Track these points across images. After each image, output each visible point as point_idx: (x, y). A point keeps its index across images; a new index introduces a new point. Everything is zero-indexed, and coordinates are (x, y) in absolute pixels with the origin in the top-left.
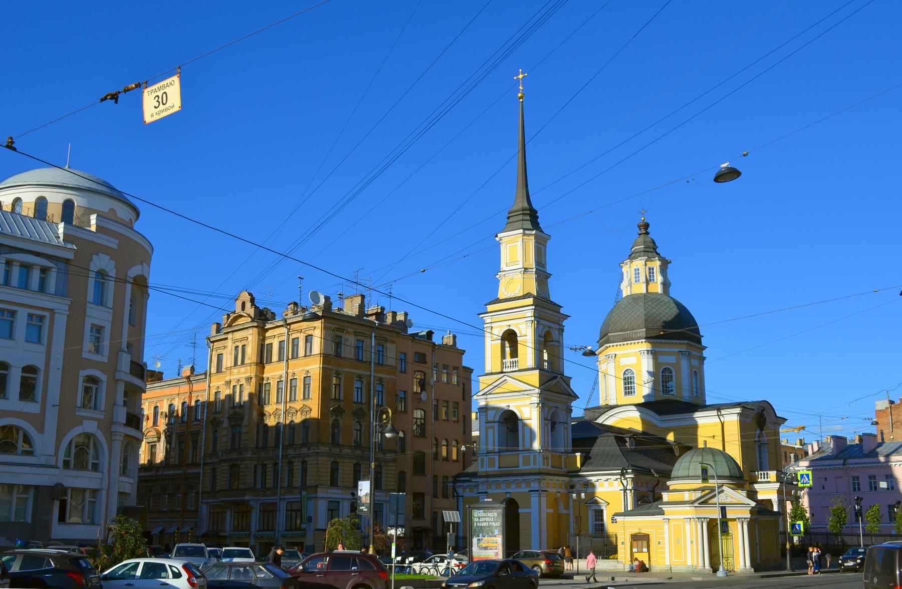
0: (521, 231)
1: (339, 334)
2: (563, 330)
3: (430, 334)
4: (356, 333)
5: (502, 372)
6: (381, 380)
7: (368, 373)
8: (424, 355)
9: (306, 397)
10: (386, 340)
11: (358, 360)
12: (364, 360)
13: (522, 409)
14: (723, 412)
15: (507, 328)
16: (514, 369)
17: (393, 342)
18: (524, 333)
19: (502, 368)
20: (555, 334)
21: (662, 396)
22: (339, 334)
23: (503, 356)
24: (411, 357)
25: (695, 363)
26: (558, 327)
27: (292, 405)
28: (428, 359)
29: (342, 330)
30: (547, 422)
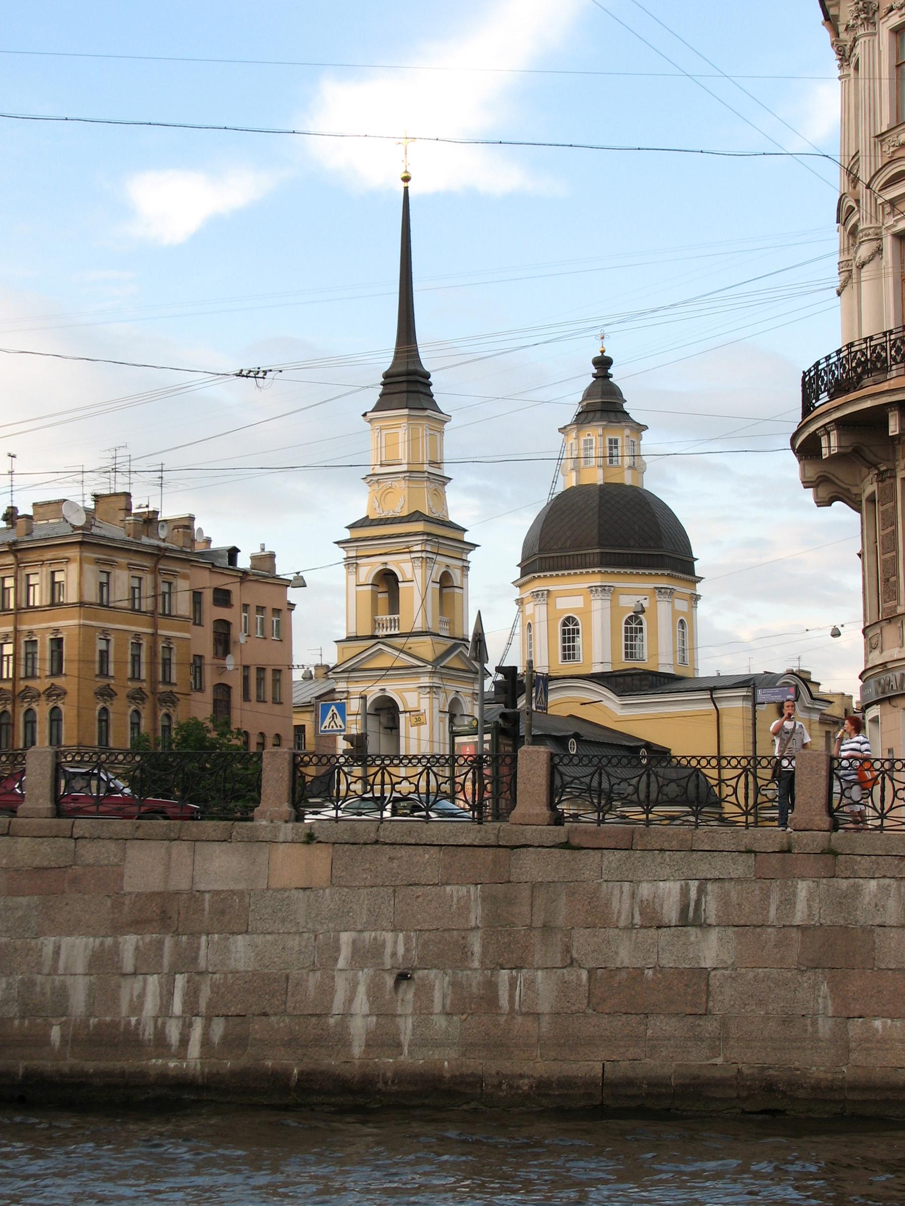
0: (405, 412)
1: (107, 569)
2: (468, 568)
3: (233, 552)
4: (130, 567)
5: (374, 637)
6: (168, 639)
7: (149, 631)
8: (228, 593)
9: (57, 671)
10: (174, 574)
11: (133, 609)
12: (143, 609)
13: (406, 695)
14: (718, 694)
15: (382, 567)
16: (393, 632)
17: (185, 577)
18: (409, 576)
19: (374, 629)
20: (456, 574)
21: (625, 664)
22: (107, 569)
23: (375, 611)
24: (208, 597)
25: (682, 605)
26: (460, 563)
27: (31, 683)
28: (235, 599)
29: (111, 563)
30: (442, 715)
